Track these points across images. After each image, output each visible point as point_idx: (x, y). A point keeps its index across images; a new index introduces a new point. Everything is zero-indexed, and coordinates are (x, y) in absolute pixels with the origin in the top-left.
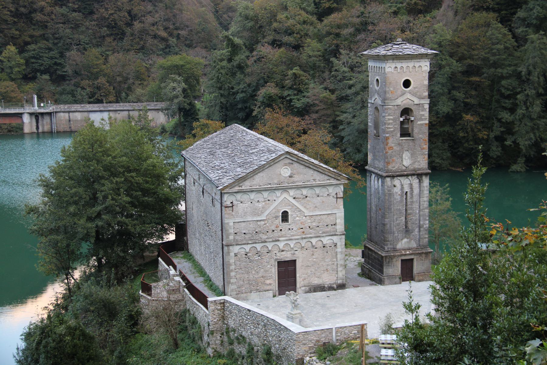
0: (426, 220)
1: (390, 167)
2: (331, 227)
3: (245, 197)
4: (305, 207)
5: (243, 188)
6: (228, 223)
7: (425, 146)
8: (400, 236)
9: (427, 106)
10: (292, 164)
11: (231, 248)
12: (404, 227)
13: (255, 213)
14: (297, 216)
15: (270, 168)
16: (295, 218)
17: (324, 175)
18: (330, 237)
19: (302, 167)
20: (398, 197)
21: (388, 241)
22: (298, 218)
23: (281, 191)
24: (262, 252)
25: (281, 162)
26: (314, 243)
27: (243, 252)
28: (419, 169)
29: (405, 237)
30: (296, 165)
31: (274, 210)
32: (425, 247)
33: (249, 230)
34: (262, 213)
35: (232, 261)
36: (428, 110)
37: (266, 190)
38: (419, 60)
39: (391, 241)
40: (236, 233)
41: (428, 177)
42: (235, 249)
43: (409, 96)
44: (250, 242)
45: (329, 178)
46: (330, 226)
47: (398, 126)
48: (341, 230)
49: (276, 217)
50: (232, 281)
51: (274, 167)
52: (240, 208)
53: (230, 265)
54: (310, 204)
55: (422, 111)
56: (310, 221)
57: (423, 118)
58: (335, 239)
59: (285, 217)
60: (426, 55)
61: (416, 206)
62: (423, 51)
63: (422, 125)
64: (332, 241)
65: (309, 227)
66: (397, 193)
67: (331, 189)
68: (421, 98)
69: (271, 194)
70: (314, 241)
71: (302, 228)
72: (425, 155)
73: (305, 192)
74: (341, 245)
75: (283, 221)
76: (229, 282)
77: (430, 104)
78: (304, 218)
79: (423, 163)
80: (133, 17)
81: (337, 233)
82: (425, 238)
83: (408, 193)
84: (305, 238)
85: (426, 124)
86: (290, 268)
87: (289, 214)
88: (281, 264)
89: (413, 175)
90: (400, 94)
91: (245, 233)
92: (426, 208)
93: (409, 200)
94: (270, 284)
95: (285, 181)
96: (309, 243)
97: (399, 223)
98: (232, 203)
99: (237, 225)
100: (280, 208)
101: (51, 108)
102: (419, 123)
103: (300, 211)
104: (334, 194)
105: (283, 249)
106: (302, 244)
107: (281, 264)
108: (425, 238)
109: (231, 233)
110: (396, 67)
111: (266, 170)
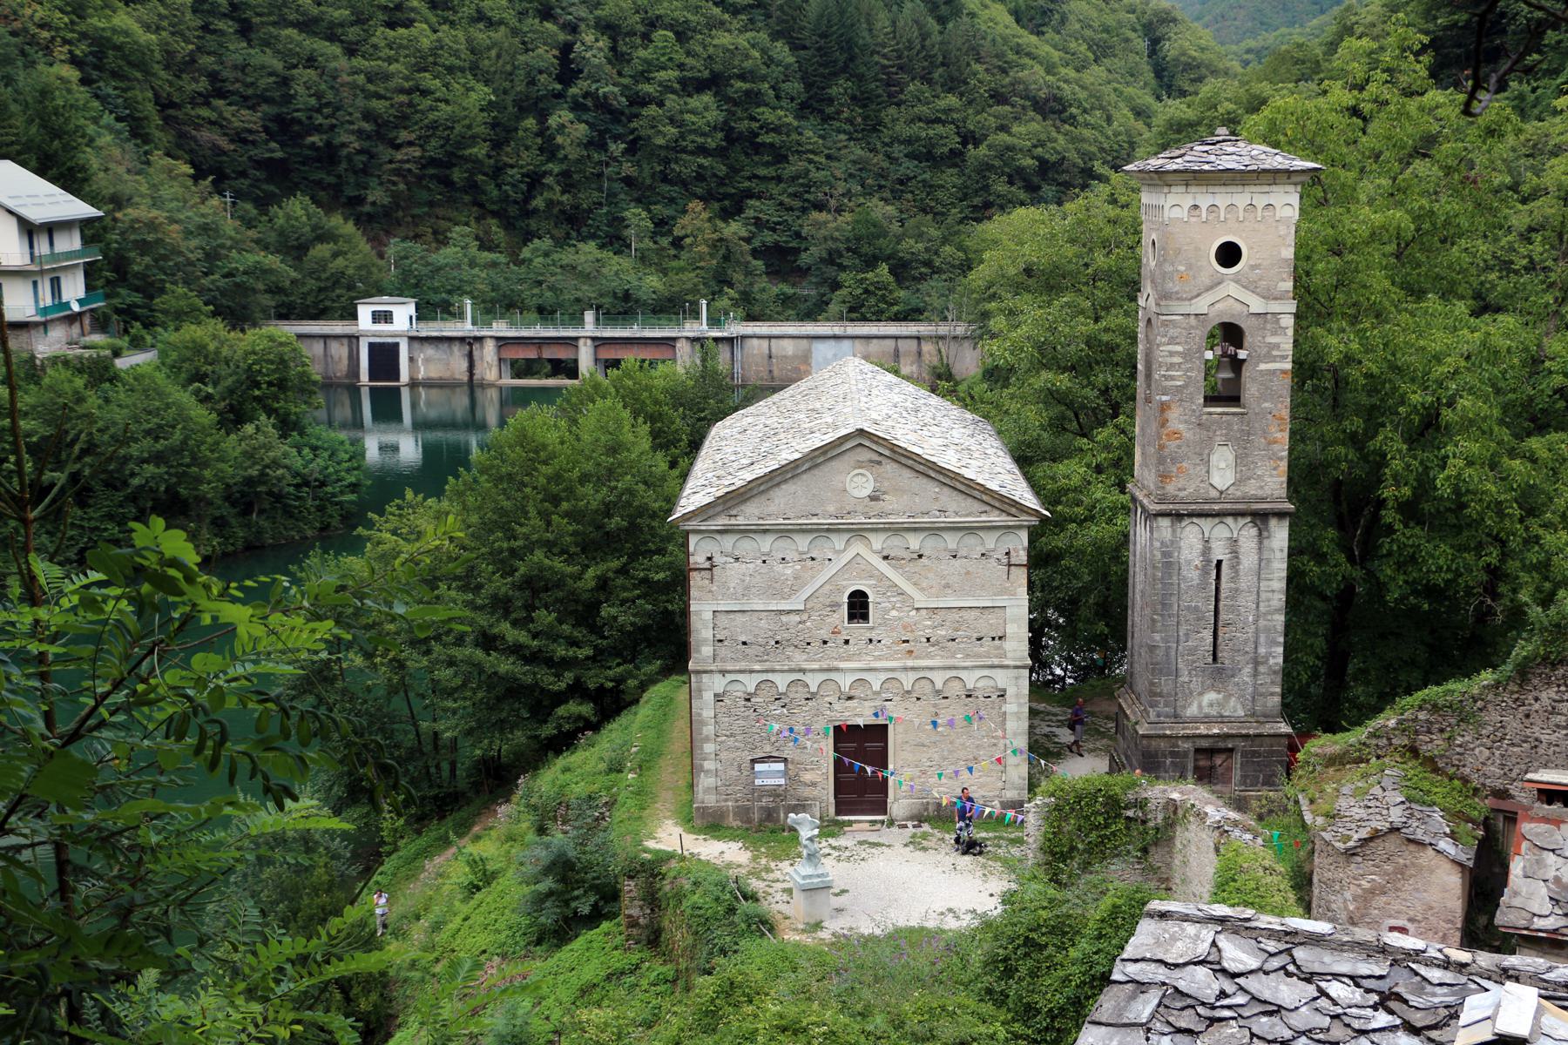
0: (1277, 644)
1: (1171, 488)
3: (746, 546)
5: (741, 520)
6: (698, 613)
7: (1279, 435)
8: (1196, 684)
9: (1288, 322)
10: (879, 463)
11: (705, 678)
12: (1210, 660)
13: (775, 589)
15: (816, 472)
16: (887, 611)
17: (970, 500)
18: (986, 672)
19: (907, 473)
20: (1193, 575)
21: (1160, 695)
22: (894, 613)
23: (846, 536)
24: (792, 695)
25: (846, 457)
26: (939, 685)
27: (738, 691)
28: (1262, 500)
29: (1213, 687)
30: (889, 468)
31: (828, 587)
32: (1268, 717)
33: (756, 636)
34: (794, 591)
35: (708, 713)
36: (1290, 332)
37: (803, 530)
38: (1266, 188)
39: (1169, 695)
41: (1286, 523)
42: (718, 683)
43: (1233, 289)
44: (757, 667)
45: (988, 508)
46: (987, 642)
47: (1198, 375)
48: (1018, 654)
49: (835, 606)
50: (708, 765)
51: (826, 468)
52: (732, 573)
53: (703, 723)
55: (1274, 334)
57: (1275, 353)
58: (1002, 679)
59: (858, 606)
60: (1287, 175)
61: (1246, 602)
62: (1278, 161)
63: (1274, 372)
64: (991, 683)
66: (1189, 562)
67: (990, 540)
68: (1268, 296)
69: (819, 542)
70: (939, 679)
72: (1281, 459)
73: (914, 541)
74: (1017, 696)
75: (852, 617)
76: (701, 769)
77: (1298, 316)
78: (913, 613)
79: (1272, 483)
80: (970, 138)
81: (1006, 662)
82: (1272, 694)
83: (1224, 566)
84: (913, 669)
85: (1284, 372)
86: (872, 745)
88: (845, 735)
89: (1236, 514)
90: (1208, 282)
92: (1277, 611)
93: (1224, 585)
94: (814, 784)
95: (859, 508)
96: (923, 682)
97: (1196, 648)
98: (709, 559)
99: (723, 620)
101: (735, 329)
102: (1263, 367)
104: (1000, 554)
105: (853, 693)
107: (845, 735)
108: (1272, 694)
109: (706, 640)
110: (1196, 207)
111: (805, 477)
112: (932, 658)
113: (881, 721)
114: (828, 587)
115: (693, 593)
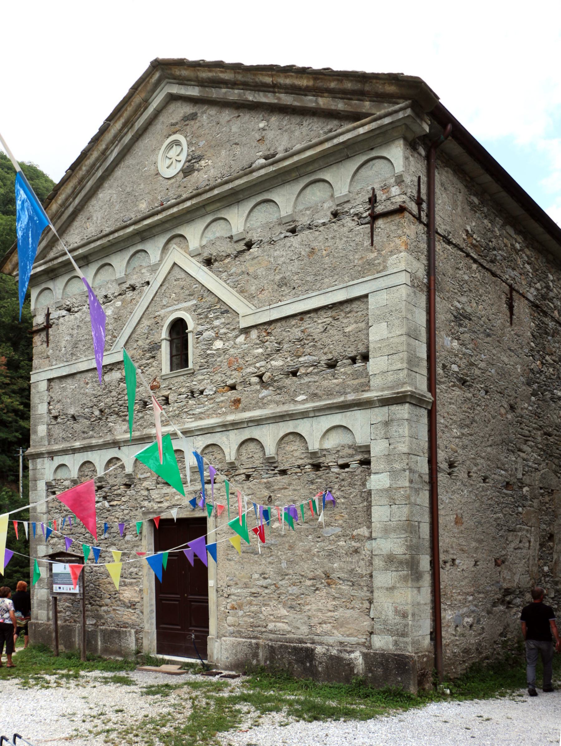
2: (349, 370)
4: (241, 292)
14: (218, 337)
16: (210, 342)
18: (337, 419)
22: (218, 344)
31: (146, 323)
33: (83, 406)
40: (56, 418)
46: (343, 369)
54: (261, 272)
56: (260, 350)
65: (260, 377)
69: (136, 262)
71: (233, 387)
74: (389, 457)
78: (242, 338)
81: (366, 395)
84: (235, 425)
87: (191, 325)
91: (74, 418)
96: (252, 446)
100: (162, 312)
103: (227, 310)
106: (226, 451)
112: (264, 406)
113: (198, 514)
114: (146, 323)
115: (35, 362)
